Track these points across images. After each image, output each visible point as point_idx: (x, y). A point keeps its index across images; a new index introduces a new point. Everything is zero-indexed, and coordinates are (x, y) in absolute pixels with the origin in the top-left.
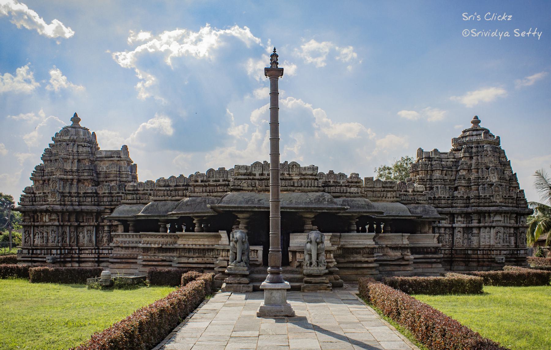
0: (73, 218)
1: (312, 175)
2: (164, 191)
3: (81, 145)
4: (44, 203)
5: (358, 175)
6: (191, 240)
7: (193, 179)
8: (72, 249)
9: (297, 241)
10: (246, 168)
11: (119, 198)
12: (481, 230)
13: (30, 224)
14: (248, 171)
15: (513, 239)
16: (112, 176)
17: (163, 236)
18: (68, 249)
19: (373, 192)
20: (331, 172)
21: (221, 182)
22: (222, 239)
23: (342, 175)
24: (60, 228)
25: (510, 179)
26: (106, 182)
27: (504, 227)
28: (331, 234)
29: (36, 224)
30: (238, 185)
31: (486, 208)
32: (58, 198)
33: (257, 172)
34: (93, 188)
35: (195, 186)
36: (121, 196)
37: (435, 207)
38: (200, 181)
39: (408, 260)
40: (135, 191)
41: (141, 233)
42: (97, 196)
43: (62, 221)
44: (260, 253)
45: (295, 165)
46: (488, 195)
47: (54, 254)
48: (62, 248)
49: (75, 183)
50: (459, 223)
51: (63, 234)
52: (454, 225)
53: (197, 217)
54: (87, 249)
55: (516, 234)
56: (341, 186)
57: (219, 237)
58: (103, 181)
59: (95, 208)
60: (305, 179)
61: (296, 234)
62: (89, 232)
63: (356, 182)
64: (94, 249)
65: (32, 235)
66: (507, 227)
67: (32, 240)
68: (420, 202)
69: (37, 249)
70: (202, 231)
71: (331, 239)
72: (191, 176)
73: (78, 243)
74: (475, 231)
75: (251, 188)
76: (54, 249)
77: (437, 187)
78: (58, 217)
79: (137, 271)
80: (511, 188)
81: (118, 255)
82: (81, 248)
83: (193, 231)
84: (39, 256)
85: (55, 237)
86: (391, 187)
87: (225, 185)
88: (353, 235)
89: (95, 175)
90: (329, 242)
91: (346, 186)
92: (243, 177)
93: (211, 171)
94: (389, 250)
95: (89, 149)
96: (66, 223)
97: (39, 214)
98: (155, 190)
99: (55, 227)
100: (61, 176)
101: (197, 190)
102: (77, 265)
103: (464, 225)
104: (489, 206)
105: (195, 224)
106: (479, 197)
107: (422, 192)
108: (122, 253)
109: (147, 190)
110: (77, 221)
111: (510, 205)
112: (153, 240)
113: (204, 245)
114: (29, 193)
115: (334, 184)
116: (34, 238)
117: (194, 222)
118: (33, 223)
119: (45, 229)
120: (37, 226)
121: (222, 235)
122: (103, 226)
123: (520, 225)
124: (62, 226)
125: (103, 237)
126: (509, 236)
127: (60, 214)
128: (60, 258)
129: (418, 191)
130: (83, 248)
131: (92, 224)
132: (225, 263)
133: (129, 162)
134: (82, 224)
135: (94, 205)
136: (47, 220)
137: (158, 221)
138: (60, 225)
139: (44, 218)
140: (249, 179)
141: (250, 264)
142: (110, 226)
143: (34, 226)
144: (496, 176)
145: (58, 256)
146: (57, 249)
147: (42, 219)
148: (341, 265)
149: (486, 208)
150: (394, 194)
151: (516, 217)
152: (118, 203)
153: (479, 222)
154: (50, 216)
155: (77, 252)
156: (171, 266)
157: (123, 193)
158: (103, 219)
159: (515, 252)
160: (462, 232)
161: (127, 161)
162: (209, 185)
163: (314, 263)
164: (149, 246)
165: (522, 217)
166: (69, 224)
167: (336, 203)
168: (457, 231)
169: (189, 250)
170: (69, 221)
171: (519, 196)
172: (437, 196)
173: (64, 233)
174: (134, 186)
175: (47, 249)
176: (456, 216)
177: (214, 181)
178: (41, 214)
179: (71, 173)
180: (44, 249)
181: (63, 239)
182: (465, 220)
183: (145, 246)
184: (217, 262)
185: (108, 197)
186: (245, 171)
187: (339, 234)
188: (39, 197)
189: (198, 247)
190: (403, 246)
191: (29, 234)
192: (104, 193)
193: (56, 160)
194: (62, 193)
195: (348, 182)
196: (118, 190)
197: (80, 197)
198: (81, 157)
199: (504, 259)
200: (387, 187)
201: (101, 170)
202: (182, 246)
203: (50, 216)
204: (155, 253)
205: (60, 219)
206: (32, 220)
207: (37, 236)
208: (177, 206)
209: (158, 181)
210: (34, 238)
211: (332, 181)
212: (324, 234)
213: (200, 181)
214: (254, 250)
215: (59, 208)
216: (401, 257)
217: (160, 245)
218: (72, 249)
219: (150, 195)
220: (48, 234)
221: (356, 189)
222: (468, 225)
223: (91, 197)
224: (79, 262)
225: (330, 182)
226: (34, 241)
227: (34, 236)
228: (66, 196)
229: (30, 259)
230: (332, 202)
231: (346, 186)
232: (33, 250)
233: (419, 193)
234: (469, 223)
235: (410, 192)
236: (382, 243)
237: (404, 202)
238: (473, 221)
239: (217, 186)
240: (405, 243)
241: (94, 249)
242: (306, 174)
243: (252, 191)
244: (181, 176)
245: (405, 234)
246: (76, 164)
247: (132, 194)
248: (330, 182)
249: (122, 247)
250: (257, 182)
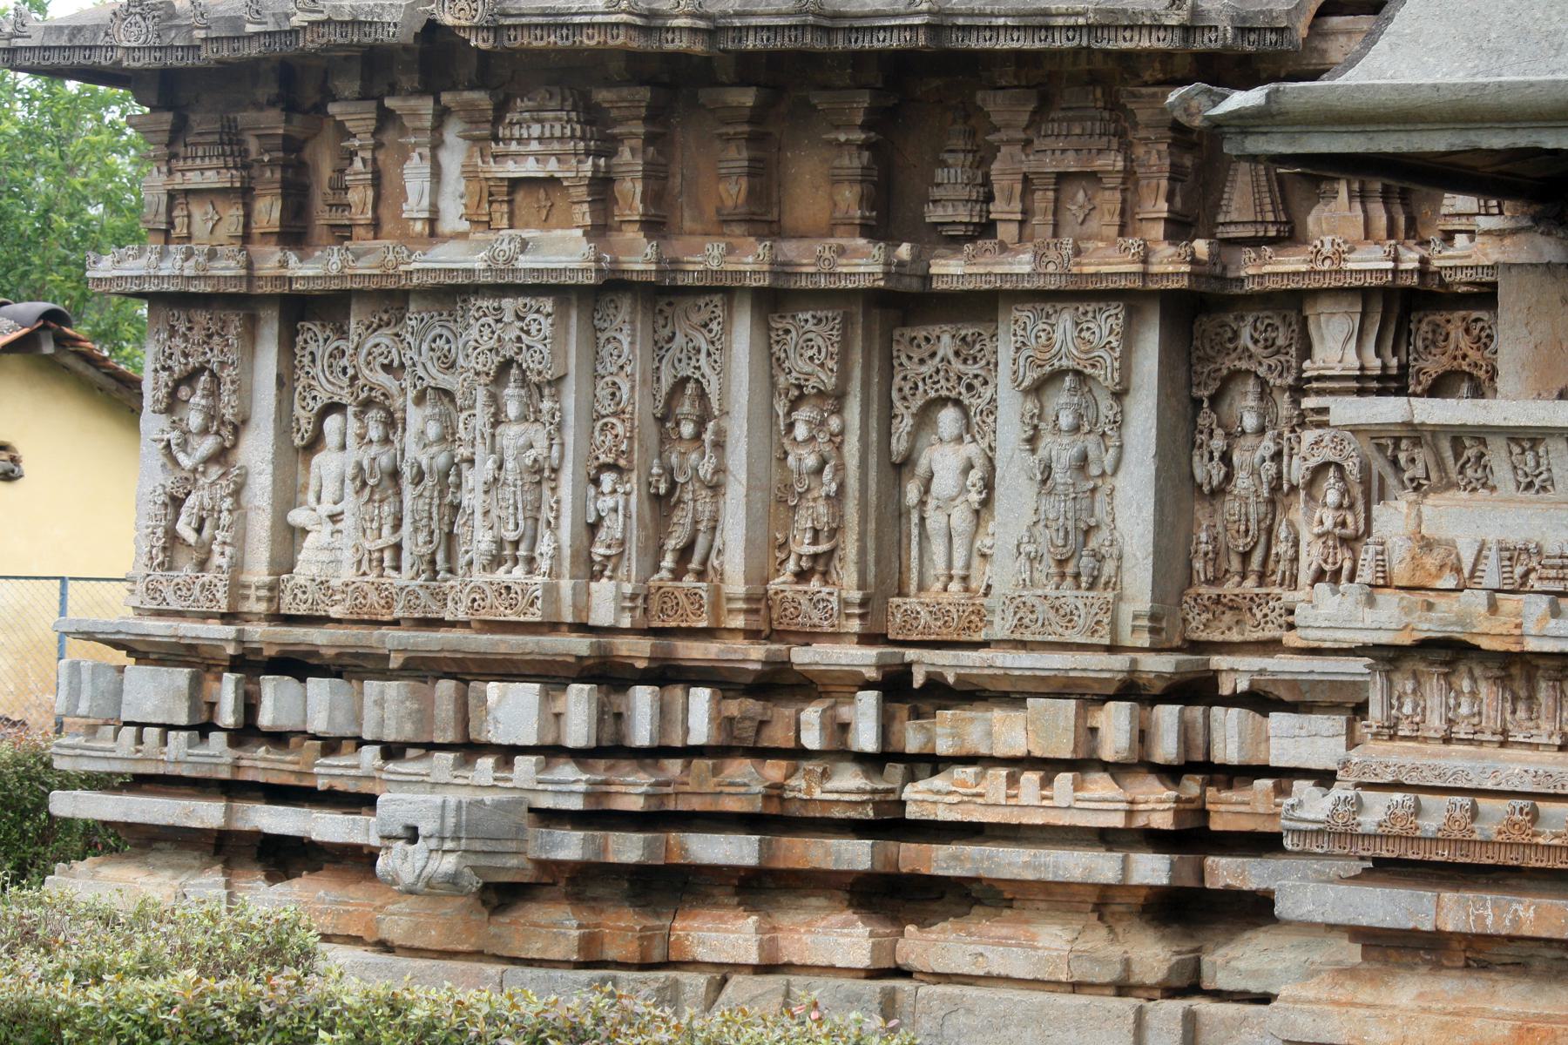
8: (781, 684)
13: (228, 267)
18: (721, 680)
24: (626, 335)
43: (654, 226)
47: (507, 754)
48: (637, 650)
51: (666, 418)
62: (1061, 402)
64: (1130, 690)
65: (257, 451)
67: (261, 525)
69: (297, 665)
73: (887, 579)
76: (508, 670)
78: (600, 136)
81: (1437, 815)
82: (924, 664)
84: (328, 772)
85: (541, 474)
97: (355, 117)
99: (542, 316)
102: (847, 939)
108: (1515, 768)
110: (879, 229)
116: (288, 494)
118: (272, 261)
119: (416, 341)
124: (661, 296)
125: (1278, 494)
127: (626, 102)
128: (598, 817)
130: (951, 664)
136: (453, 218)
139: (414, 179)
145: (569, 786)
146: (552, 676)
154: (489, 133)
155: (866, 738)
166: (751, 260)
170: (763, 217)
173: (682, 407)
175: (421, 669)
178: (386, 118)
181: (663, 503)
203: (489, 133)
205: (631, 192)
206: (269, 211)
207: (328, 465)
210: (288, 494)
218: (781, 684)
220: (448, 436)
224: (891, 897)
226: (289, 537)
229: (208, 814)
232: (250, 664)
241: (1130, 690)
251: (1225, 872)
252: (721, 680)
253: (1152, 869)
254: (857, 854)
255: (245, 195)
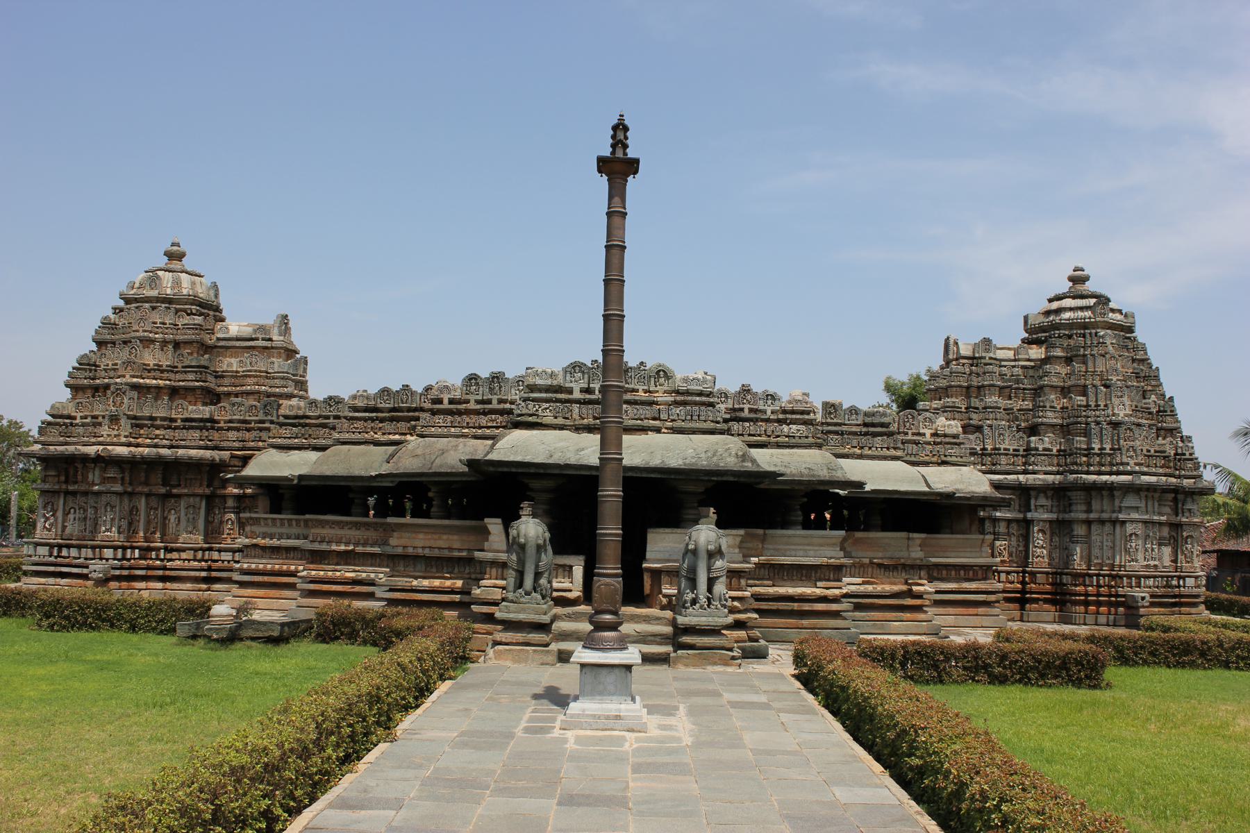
0: (157, 477)
1: (700, 394)
2: (365, 420)
3: (185, 311)
4: (93, 440)
5: (807, 395)
6: (421, 536)
7: (434, 394)
9: (662, 547)
10: (552, 375)
11: (264, 435)
12: (1094, 527)
13: (57, 487)
14: (555, 383)
15: (1167, 551)
16: (249, 381)
17: (357, 526)
18: (140, 548)
19: (842, 434)
20: (746, 390)
21: (495, 405)
22: (491, 538)
23: (773, 397)
24: (126, 501)
25: (1159, 411)
26: (236, 395)
27: (1145, 522)
28: (742, 532)
29: (71, 488)
30: (531, 415)
31: (1105, 478)
32: (125, 426)
33: (576, 385)
34: (207, 409)
35: (434, 413)
36: (268, 429)
37: (984, 472)
38: (446, 401)
39: (919, 596)
40: (298, 421)
41: (307, 516)
42: (213, 428)
43: (130, 484)
44: (578, 571)
45: (662, 373)
46: (1108, 446)
47: (107, 560)
49: (166, 398)
50: (1041, 510)
51: (131, 511)
52: (1029, 515)
53: (436, 483)
54: (184, 550)
55: (1176, 540)
56: (768, 420)
57: (485, 532)
58: (229, 394)
59: (208, 454)
60: (684, 403)
61: (661, 530)
63: (802, 413)
64: (201, 549)
65: (60, 514)
66: (1153, 523)
67: (60, 526)
68: (949, 459)
69: (69, 547)
70: (448, 517)
71: (741, 542)
72: (428, 389)
74: (1080, 530)
75: (560, 421)
77: (990, 426)
78: (123, 472)
79: (292, 604)
80: (1162, 432)
83: (426, 515)
86: (882, 425)
87: (502, 412)
88: (794, 536)
89: (210, 378)
90: (737, 550)
91: (779, 421)
92: (544, 395)
93: (472, 379)
94: (876, 571)
95: (199, 320)
96: (140, 489)
97: (79, 466)
98: (345, 418)
100: (135, 380)
101: (439, 419)
102: (160, 585)
103: (1054, 516)
104: (1111, 473)
105: (432, 499)
106: (1088, 452)
107: (955, 436)
109: (327, 417)
111: (1161, 471)
112: (336, 533)
113: (450, 549)
114: (61, 417)
115: (752, 415)
116: (64, 521)
117: (430, 494)
118: (64, 486)
119: (91, 500)
120: (74, 493)
121: (490, 527)
122: (224, 497)
123: (1184, 520)
126: (1160, 545)
129: (945, 436)
131: (200, 491)
132: (497, 594)
133: (290, 353)
134: (175, 491)
135: (207, 448)
136: (97, 481)
137: (348, 489)
138: (125, 492)
139: (91, 476)
140: (558, 401)
141: (553, 599)
142: (238, 498)
143: (67, 493)
144: (1128, 403)
146: (115, 548)
147: (85, 478)
148: (764, 606)
149: (1105, 478)
150: (890, 440)
151: (1175, 500)
152: (261, 444)
153: (1089, 511)
154: (104, 470)
156: (371, 596)
157: (272, 422)
158: (225, 483)
159: (1174, 582)
160: (1048, 533)
161: (287, 350)
162: (468, 412)
163: (703, 600)
164: (324, 547)
165: (1189, 500)
166: (146, 490)
167: (754, 461)
168: (1036, 529)
169: (416, 558)
170: (146, 484)
171: (1179, 451)
172: (989, 447)
173: (134, 510)
174: (299, 408)
175: (93, 548)
176: (1033, 493)
177: (478, 402)
178: (85, 466)
179: (158, 374)
180: (86, 547)
181: (130, 524)
182: (1055, 503)
183: (316, 546)
184: (478, 591)
185: (238, 429)
186: (549, 382)
187: (760, 531)
188: (83, 425)
189: (436, 553)
190: (909, 562)
191: (54, 511)
192: (230, 421)
193: (125, 343)
194: (135, 418)
195: (784, 412)
196: (261, 417)
197: (176, 428)
198: (180, 338)
199: (1148, 598)
200: (873, 425)
201: (225, 368)
202: (400, 551)
203: (104, 470)
204: (337, 564)
205: (127, 478)
206: (63, 478)
207: (71, 516)
208: (392, 456)
209: (354, 397)
211: (746, 407)
212: (728, 532)
213: (446, 401)
214: (563, 566)
215: (123, 451)
216: (904, 588)
217: (351, 547)
218: (150, 549)
219: (334, 428)
220: (96, 512)
221: (802, 427)
222: (1061, 517)
223: (201, 429)
225: (742, 410)
226: (64, 527)
227: (66, 514)
228: (141, 426)
229: (52, 569)
230: (744, 457)
231: (779, 421)
232: (60, 547)
233: (947, 440)
234: (1065, 512)
235: (928, 435)
236: (860, 554)
237: (913, 459)
238: (1074, 508)
239: (485, 413)
240: (913, 555)
242: (688, 393)
243: (562, 427)
244: (406, 388)
245: (916, 535)
246: (170, 353)
247: (294, 425)
248: (742, 410)
249: (264, 548)
250: (576, 407)
251: (214, 574)
252: (140, 548)
253: (204, 574)
254: (160, 573)
255: (58, 476)
